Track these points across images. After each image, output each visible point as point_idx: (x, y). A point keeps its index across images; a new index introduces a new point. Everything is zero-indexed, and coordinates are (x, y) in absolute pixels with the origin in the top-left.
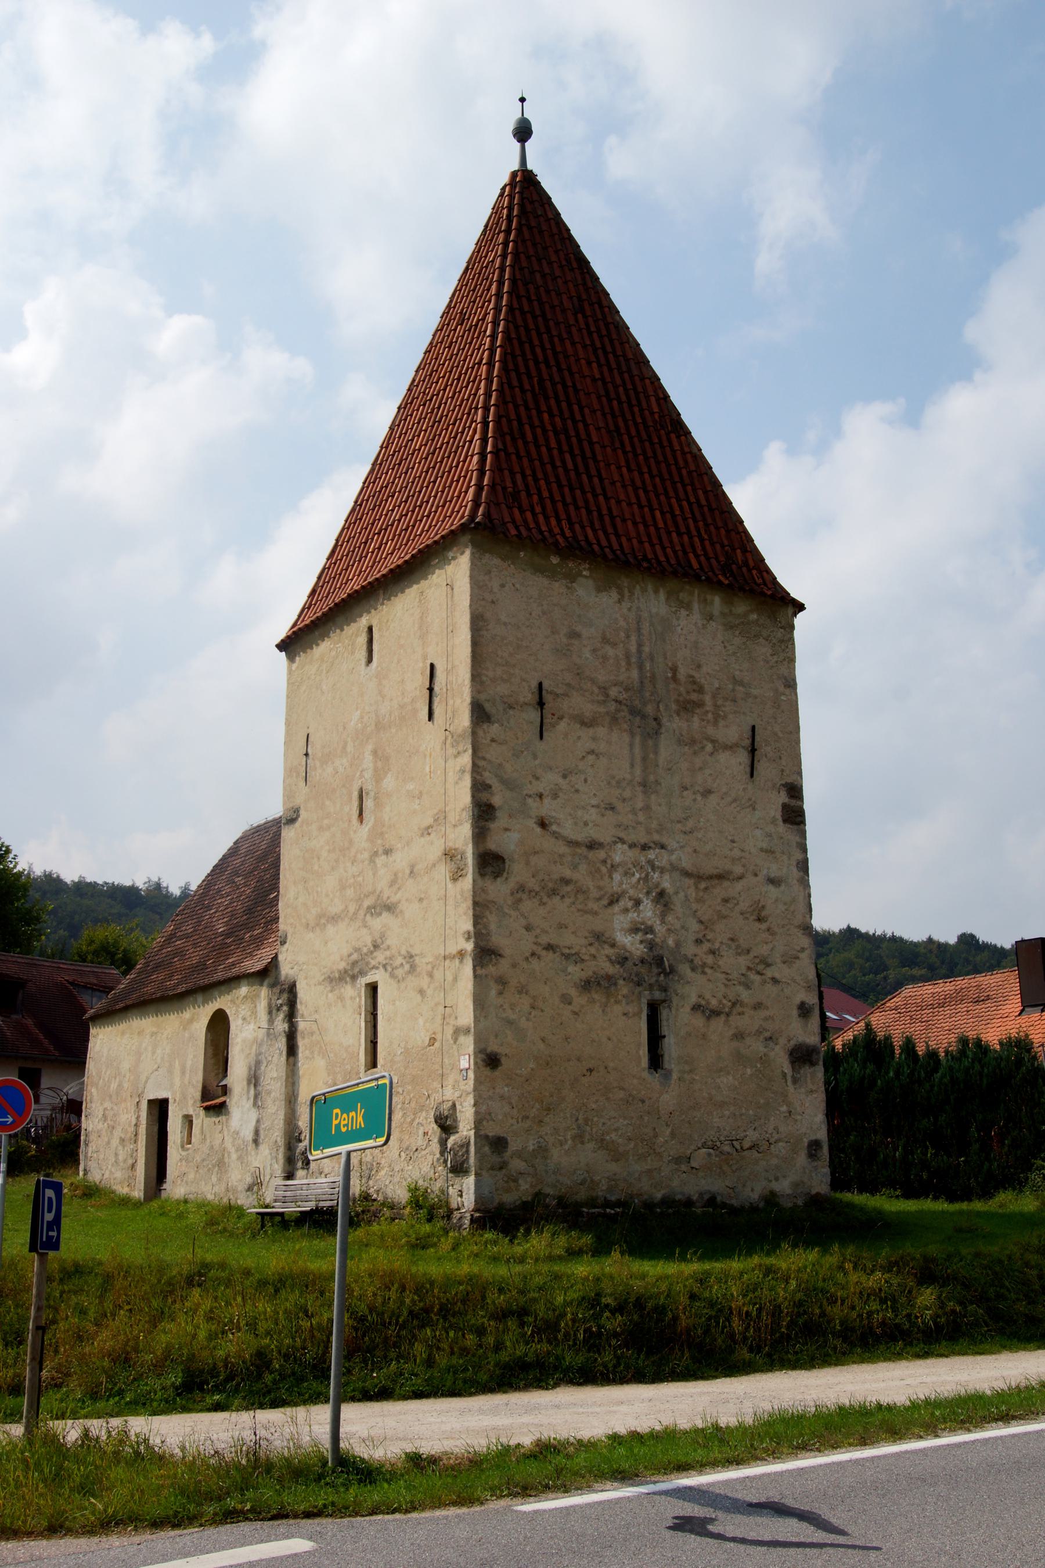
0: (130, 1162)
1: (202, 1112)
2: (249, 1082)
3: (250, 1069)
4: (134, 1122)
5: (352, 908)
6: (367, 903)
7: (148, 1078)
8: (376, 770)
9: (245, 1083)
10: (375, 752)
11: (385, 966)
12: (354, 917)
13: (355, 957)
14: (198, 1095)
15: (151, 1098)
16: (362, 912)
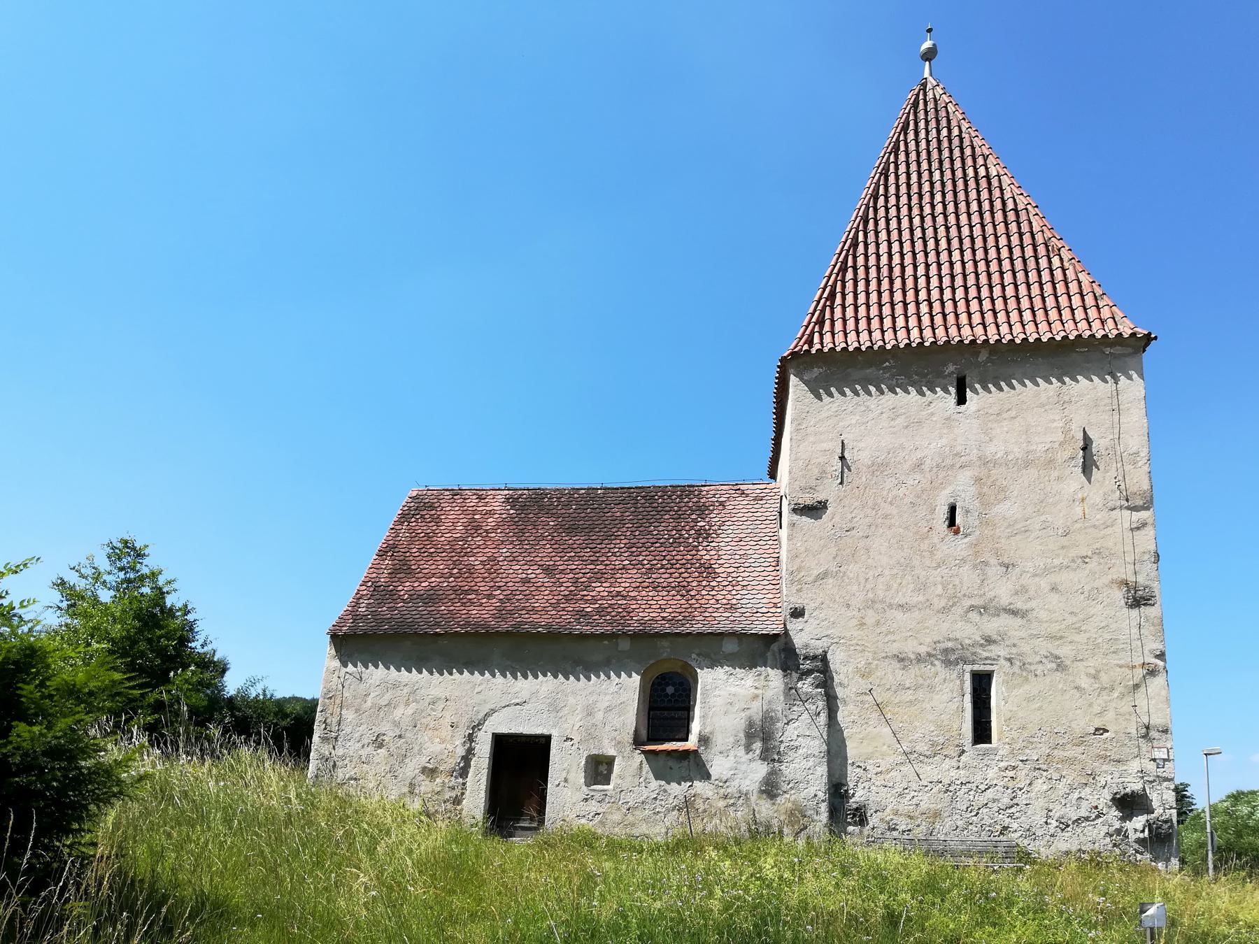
0: (448, 795)
1: (639, 758)
2: (750, 736)
3: (751, 724)
4: (461, 751)
5: (939, 604)
6: (967, 603)
7: (494, 711)
8: (981, 495)
9: (742, 735)
10: (978, 480)
11: (1010, 660)
12: (945, 610)
13: (950, 645)
14: (628, 737)
15: (504, 730)
16: (959, 610)
